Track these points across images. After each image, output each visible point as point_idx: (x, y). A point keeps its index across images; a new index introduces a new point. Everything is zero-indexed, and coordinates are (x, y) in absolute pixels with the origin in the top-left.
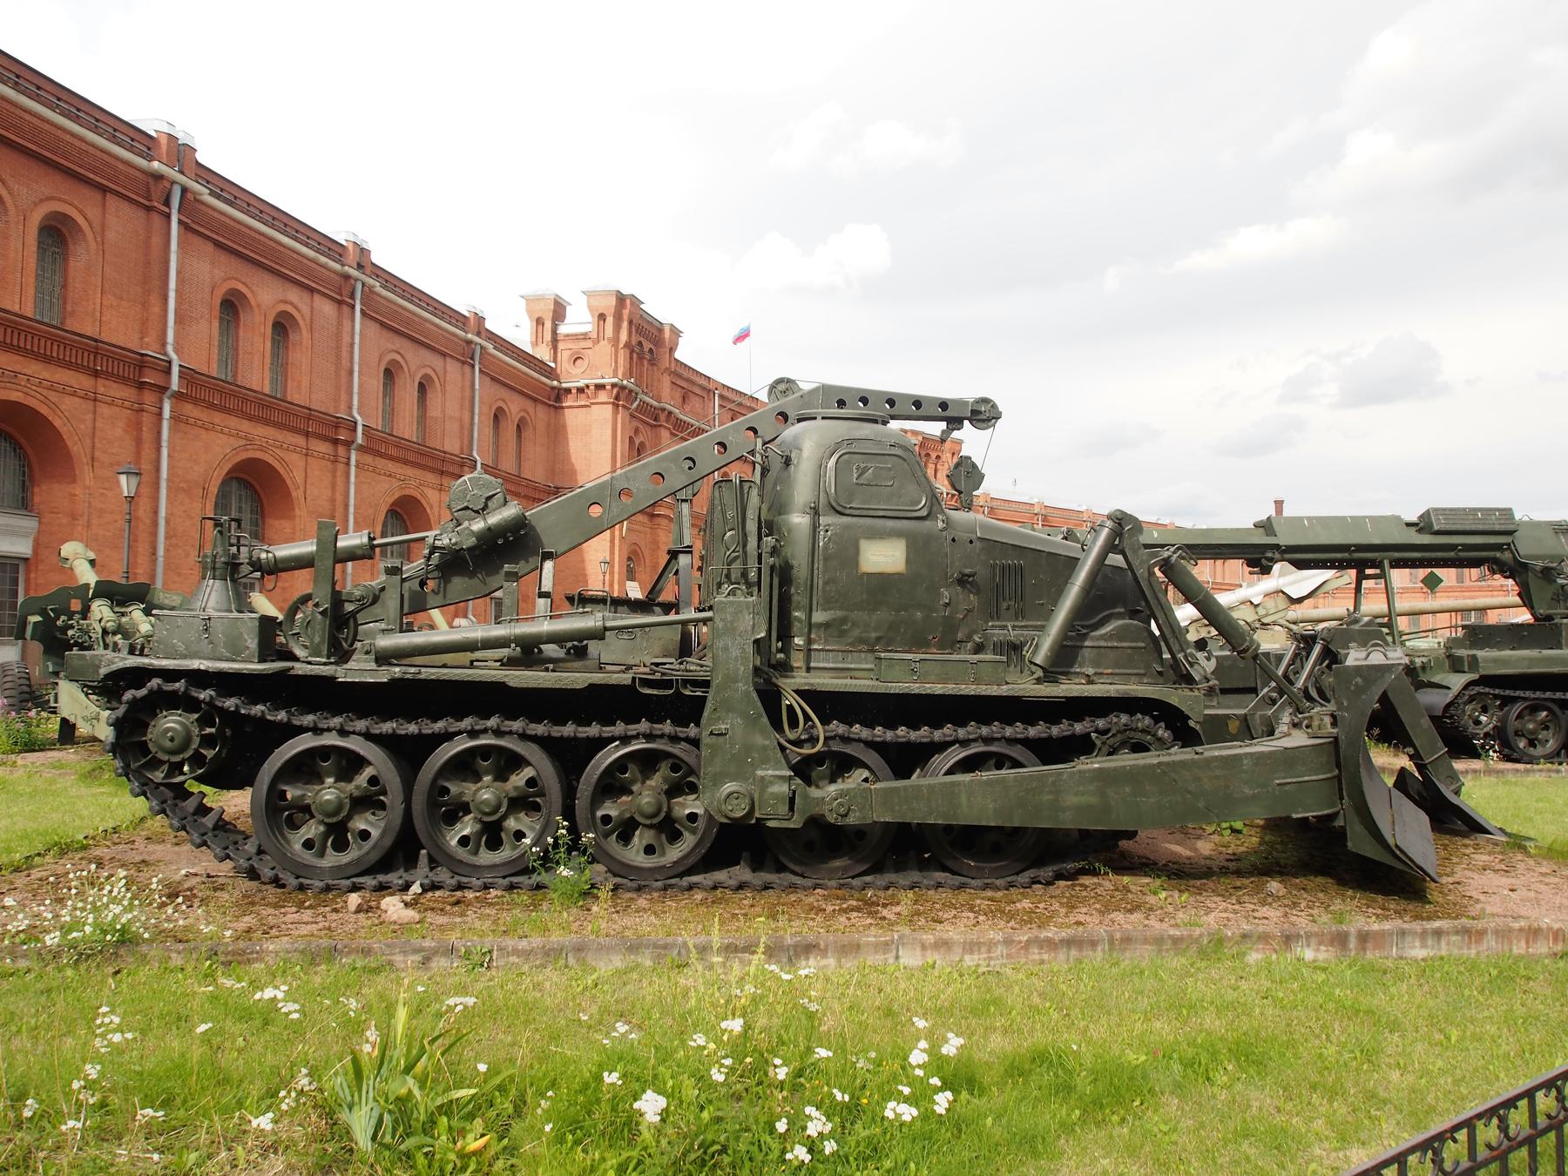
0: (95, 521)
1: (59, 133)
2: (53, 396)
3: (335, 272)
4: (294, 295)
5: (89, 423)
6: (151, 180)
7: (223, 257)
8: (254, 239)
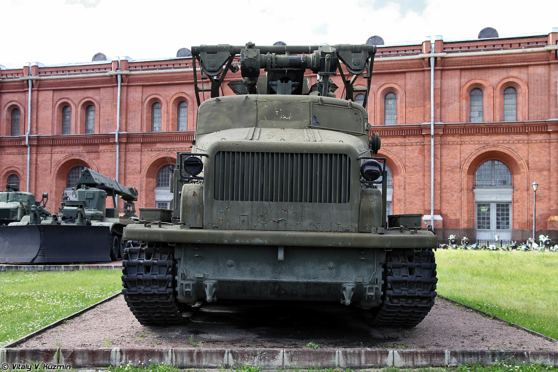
0: (407, 187)
1: (383, 63)
2: (388, 148)
3: (544, 52)
4: (514, 73)
5: (403, 154)
6: (422, 61)
7: (466, 74)
8: (482, 59)
